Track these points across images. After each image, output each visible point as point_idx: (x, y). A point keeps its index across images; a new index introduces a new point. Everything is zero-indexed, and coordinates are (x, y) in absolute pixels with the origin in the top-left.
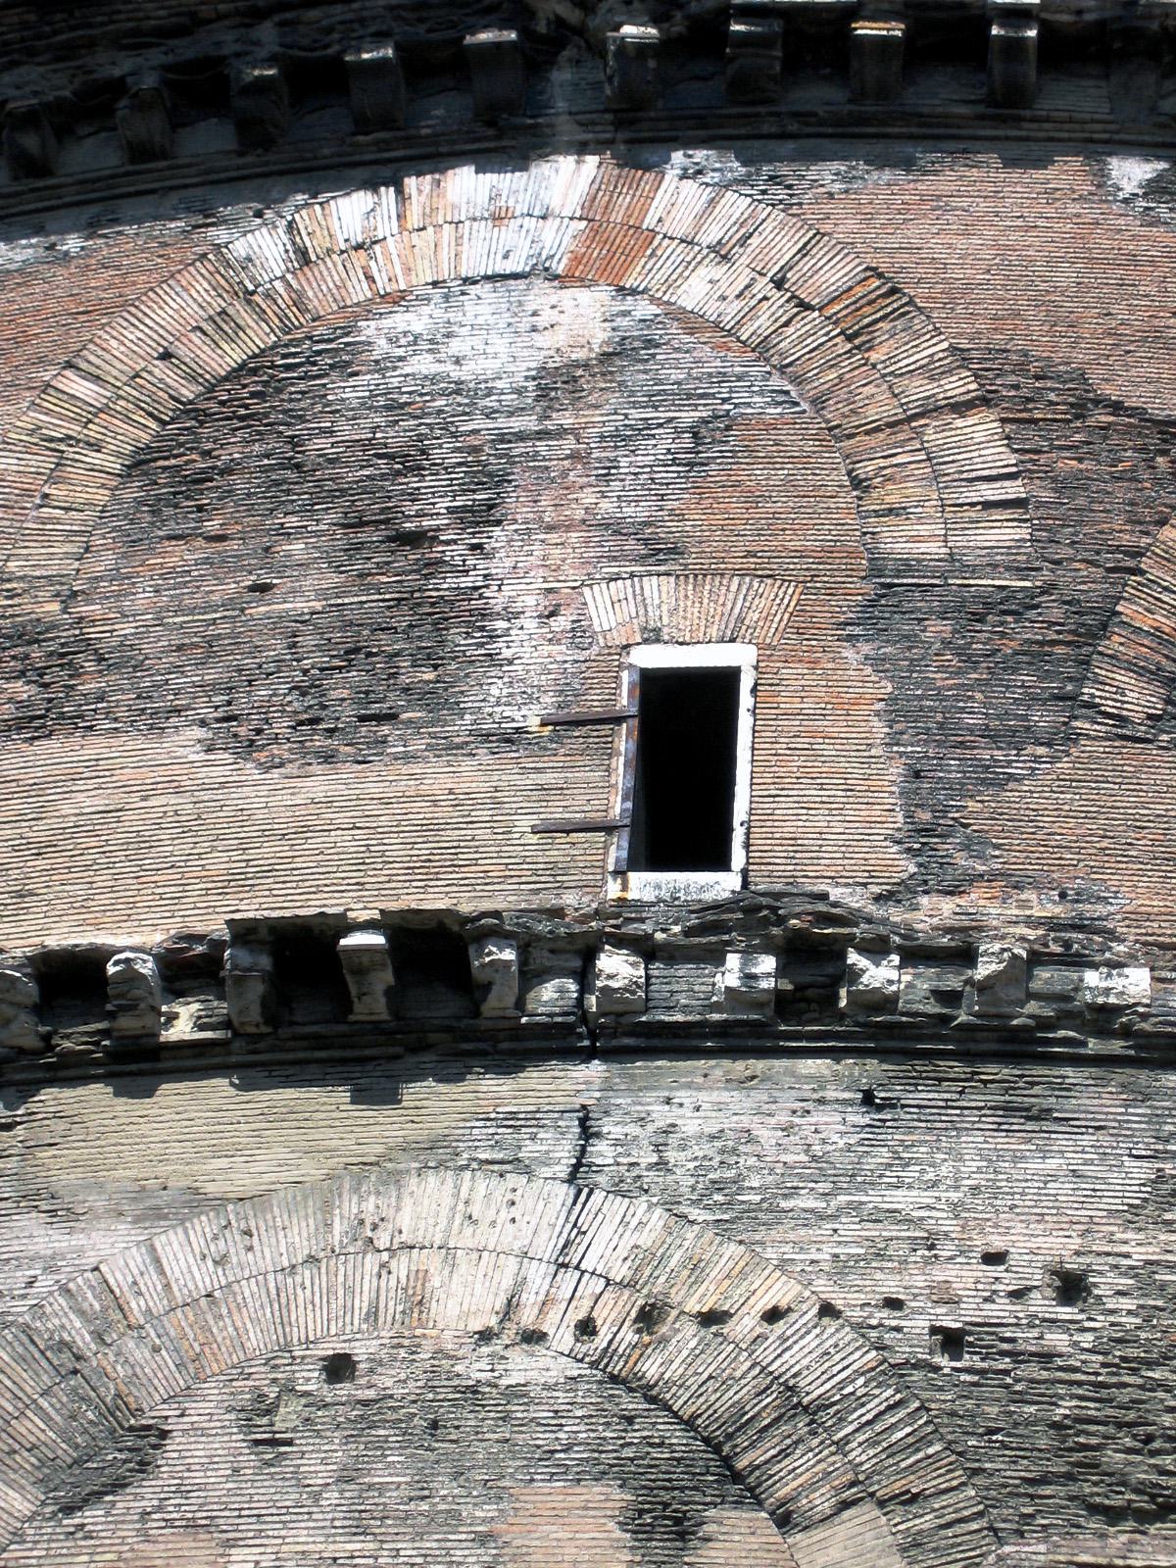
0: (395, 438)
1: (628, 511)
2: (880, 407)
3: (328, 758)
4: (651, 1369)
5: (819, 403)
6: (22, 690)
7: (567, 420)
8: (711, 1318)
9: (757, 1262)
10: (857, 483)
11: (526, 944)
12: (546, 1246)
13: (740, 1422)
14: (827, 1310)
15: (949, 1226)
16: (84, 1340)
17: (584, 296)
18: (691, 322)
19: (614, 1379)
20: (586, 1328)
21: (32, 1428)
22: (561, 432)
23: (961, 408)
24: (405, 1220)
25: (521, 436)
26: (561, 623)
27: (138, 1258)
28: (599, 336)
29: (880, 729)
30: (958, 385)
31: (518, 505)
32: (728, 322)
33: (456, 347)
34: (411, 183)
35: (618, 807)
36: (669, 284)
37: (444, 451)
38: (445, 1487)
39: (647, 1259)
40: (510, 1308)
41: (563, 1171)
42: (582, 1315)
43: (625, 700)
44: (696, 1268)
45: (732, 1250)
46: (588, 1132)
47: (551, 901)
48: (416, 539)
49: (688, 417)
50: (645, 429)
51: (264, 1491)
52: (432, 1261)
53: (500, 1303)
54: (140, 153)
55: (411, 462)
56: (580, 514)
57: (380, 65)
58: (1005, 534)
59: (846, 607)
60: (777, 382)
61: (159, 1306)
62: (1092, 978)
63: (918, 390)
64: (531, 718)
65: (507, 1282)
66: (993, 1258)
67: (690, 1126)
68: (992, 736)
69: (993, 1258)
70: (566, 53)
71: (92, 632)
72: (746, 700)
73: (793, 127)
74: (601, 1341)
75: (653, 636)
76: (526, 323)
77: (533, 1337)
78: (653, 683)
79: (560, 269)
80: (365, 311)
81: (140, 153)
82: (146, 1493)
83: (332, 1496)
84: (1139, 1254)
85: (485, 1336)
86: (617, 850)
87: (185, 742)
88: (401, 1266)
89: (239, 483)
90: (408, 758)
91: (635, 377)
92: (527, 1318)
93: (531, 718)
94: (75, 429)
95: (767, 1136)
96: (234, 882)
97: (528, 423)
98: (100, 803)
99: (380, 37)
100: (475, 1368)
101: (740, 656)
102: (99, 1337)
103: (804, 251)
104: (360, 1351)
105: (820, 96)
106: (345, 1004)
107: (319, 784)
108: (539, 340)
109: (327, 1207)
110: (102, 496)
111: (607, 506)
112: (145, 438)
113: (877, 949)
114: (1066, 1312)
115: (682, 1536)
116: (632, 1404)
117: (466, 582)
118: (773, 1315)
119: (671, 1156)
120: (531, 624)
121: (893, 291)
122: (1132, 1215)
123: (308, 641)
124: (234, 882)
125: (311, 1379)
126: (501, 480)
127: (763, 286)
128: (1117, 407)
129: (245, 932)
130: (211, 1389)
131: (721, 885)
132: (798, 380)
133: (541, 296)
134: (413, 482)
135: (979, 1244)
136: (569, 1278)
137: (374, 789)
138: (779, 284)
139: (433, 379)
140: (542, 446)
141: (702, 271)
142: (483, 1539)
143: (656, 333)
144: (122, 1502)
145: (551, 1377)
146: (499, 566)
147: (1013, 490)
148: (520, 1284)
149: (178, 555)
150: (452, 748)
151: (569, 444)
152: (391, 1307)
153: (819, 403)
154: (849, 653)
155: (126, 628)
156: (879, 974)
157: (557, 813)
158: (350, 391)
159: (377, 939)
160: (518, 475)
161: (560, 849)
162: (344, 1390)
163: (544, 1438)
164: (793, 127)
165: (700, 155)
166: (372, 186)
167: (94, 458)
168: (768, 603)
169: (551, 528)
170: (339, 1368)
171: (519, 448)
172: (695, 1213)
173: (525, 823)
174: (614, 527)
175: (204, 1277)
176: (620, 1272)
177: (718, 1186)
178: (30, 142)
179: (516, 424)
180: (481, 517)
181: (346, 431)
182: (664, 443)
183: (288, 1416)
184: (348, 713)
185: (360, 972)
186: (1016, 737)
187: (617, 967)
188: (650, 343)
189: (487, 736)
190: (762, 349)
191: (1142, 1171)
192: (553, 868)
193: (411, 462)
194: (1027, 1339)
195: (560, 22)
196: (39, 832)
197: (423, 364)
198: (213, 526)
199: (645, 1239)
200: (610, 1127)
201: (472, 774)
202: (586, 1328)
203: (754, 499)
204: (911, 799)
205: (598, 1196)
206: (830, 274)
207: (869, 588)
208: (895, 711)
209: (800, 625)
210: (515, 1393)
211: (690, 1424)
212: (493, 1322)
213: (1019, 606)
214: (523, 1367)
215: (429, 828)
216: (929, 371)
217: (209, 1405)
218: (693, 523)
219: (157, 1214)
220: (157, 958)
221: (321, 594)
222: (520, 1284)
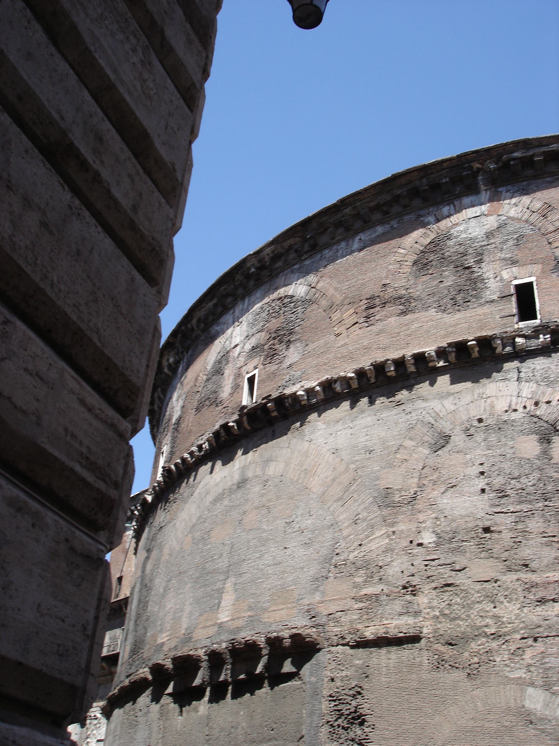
0: (461, 250)
1: (507, 256)
3: (459, 311)
4: (538, 413)
5: (539, 229)
6: (401, 307)
7: (492, 241)
8: (548, 402)
10: (549, 243)
12: (515, 393)
16: (433, 422)
17: (492, 218)
18: (512, 219)
19: (532, 416)
20: (525, 407)
21: (426, 438)
22: (492, 243)
24: (488, 392)
25: (484, 246)
26: (498, 279)
27: (440, 406)
28: (496, 225)
31: (486, 258)
32: (519, 217)
33: (469, 231)
34: (456, 203)
35: (515, 311)
36: (507, 212)
37: (470, 251)
38: (503, 440)
39: (533, 393)
40: (510, 407)
41: (516, 379)
42: (523, 405)
43: (513, 291)
44: (544, 393)
45: (550, 389)
47: (505, 330)
48: (468, 268)
49: (515, 237)
50: (507, 240)
51: (470, 444)
52: (494, 399)
53: (508, 405)
54: (405, 207)
55: (464, 254)
56: (498, 258)
57: (446, 182)
60: (531, 227)
61: (445, 414)
65: (509, 401)
67: (538, 367)
70: (480, 174)
71: (412, 295)
72: (535, 287)
73: (525, 179)
74: (528, 409)
75: (516, 278)
76: (481, 225)
77: (515, 410)
78: (517, 287)
79: (486, 213)
80: (452, 227)
81: (405, 207)
82: (448, 447)
83: (483, 444)
85: (506, 411)
86: (516, 319)
87: (432, 312)
88: (489, 401)
89: (433, 263)
90: (474, 308)
91: (503, 230)
92: (513, 407)
93: (495, 297)
94: (402, 259)
95: (553, 367)
96: (445, 336)
97: (485, 243)
98: (419, 325)
99: (446, 177)
100: (505, 417)
101: (532, 279)
102: (435, 420)
103: (531, 202)
104: (483, 417)
106: (470, 355)
107: (458, 315)
108: (485, 227)
109: (473, 392)
110: (409, 270)
111: (503, 256)
112: (415, 258)
115: (549, 442)
116: (536, 420)
117: (479, 274)
119: (536, 374)
120: (492, 280)
121: (550, 206)
123: (451, 290)
124: (445, 336)
125: (476, 423)
127: (525, 210)
129: (450, 345)
130: (458, 427)
131: (537, 322)
132: (535, 226)
133: (483, 219)
134: (465, 257)
136: (520, 398)
137: (469, 315)
138: (528, 208)
139: (467, 238)
140: (489, 247)
141: (513, 209)
142: (512, 448)
143: (506, 222)
144: (445, 449)
145: (520, 417)
146: (485, 270)
148: (511, 401)
149: (425, 278)
150: (482, 305)
151: (494, 246)
152: (488, 408)
153: (539, 229)
155: (418, 293)
157: (503, 314)
158: (451, 243)
159: (474, 342)
160: (485, 253)
161: (505, 320)
162: (482, 424)
163: (520, 428)
164: (525, 179)
165: (509, 187)
166: (448, 204)
167: (406, 263)
168: (537, 268)
169: (493, 262)
170: (480, 420)
171: (484, 248)
172: (542, 384)
173: (498, 317)
174: (505, 259)
175: (453, 408)
176: (530, 396)
177: (545, 378)
178: (385, 208)
179: (483, 243)
180: (480, 261)
181: (452, 250)
182: (511, 243)
183: (472, 431)
184: (461, 302)
185: (473, 349)
187: (520, 341)
188: (506, 224)
189: (487, 302)
190: (527, 221)
192: (504, 324)
193: (464, 254)
195: (478, 168)
196: (408, 332)
197: (464, 236)
198: (430, 272)
199: (533, 389)
200: (523, 370)
201: (487, 309)
202: (525, 407)
203: (530, 250)
205: (523, 383)
206: (537, 205)
207: (555, 262)
209: (543, 272)
210: (513, 421)
211: (547, 422)
212: (507, 408)
214: (514, 416)
215: (480, 320)
217: (458, 430)
218: (519, 255)
219: (442, 397)
220: (435, 352)
221: (453, 281)
222: (511, 401)
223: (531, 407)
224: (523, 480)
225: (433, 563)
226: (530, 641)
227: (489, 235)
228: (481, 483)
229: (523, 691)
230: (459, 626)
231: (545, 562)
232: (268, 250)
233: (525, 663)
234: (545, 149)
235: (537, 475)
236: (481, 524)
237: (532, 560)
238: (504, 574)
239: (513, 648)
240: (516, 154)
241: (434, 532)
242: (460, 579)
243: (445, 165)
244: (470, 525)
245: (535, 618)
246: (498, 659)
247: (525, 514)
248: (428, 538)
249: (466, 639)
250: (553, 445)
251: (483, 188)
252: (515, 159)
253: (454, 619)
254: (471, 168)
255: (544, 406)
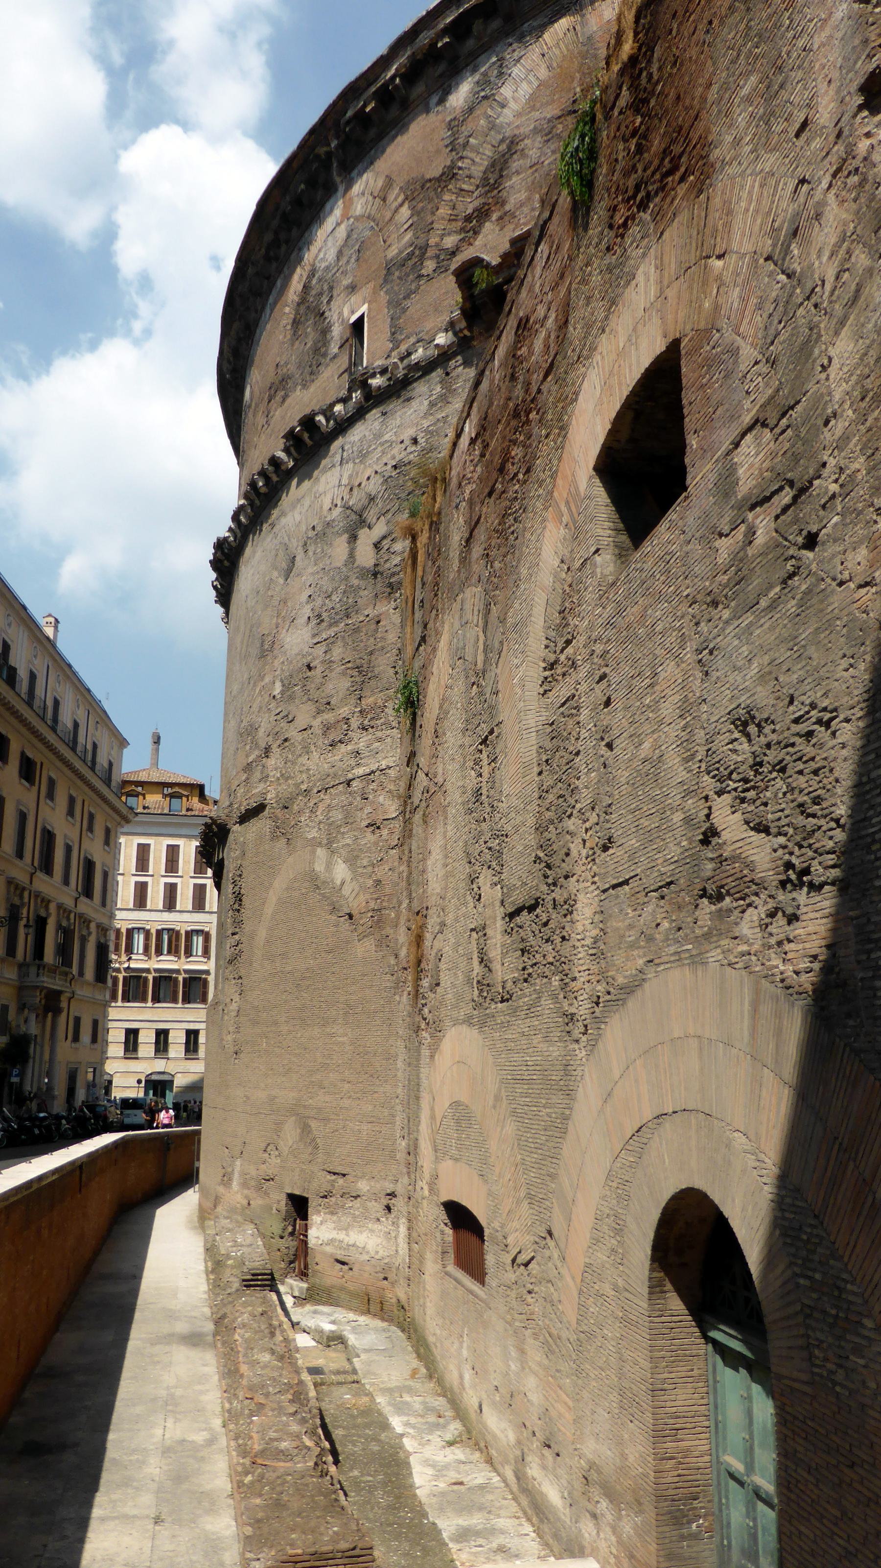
2: (388, 215)
8: (360, 485)
9: (365, 467)
11: (323, 412)
13: (365, 508)
14: (376, 472)
15: (394, 438)
18: (357, 219)
23: (401, 205)
29: (386, 310)
30: (400, 199)
31: (335, 293)
38: (325, 548)
39: (350, 476)
44: (357, 473)
46: (343, 450)
55: (321, 294)
58: (409, 236)
59: (381, 281)
60: (372, 224)
62: (413, 357)
63: (396, 204)
64: (335, 350)
66: (402, 442)
68: (404, 298)
69: (402, 442)
72: (366, 319)
75: (353, 312)
77: (336, 505)
84: (425, 425)
91: (350, 242)
95: (367, 434)
100: (328, 519)
101: (364, 309)
105: (372, 133)
113: (373, 375)
114: (414, 448)
118: (368, 478)
122: (425, 416)
126: (331, 288)
128: (430, 180)
135: (399, 440)
147: (410, 222)
149: (297, 343)
154: (382, 293)
156: (376, 382)
158: (314, 281)
163: (337, 529)
168: (371, 285)
172: (357, 461)
174: (347, 288)
182: (354, 257)
186: (407, 297)
190: (368, 217)
191: (426, 403)
194: (406, 460)
200: (346, 448)
204: (391, 327)
208: (389, 302)
210: (333, 521)
213: (411, 255)
216: (396, 199)
223: (346, 497)
224: (334, 597)
225: (279, 717)
226: (322, 795)
227: (340, 254)
228: (307, 611)
229: (313, 852)
230: (289, 786)
231: (341, 695)
232: (225, 346)
233: (317, 820)
234: (373, 89)
235: (343, 587)
236: (305, 661)
237: (332, 696)
238: (314, 717)
239: (311, 804)
240: (349, 114)
241: (282, 681)
242: (292, 733)
243: (295, 165)
244: (300, 665)
245: (326, 766)
246: (303, 819)
247: (332, 640)
248: (278, 689)
249: (292, 799)
250: (358, 542)
251: (338, 179)
252: (348, 122)
253: (287, 779)
254: (318, 156)
255: (355, 490)
